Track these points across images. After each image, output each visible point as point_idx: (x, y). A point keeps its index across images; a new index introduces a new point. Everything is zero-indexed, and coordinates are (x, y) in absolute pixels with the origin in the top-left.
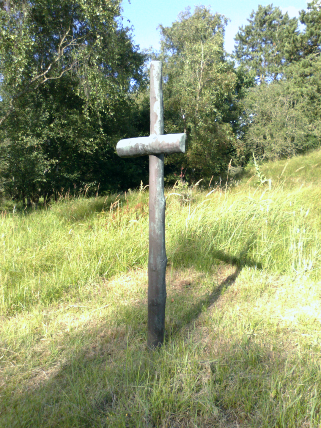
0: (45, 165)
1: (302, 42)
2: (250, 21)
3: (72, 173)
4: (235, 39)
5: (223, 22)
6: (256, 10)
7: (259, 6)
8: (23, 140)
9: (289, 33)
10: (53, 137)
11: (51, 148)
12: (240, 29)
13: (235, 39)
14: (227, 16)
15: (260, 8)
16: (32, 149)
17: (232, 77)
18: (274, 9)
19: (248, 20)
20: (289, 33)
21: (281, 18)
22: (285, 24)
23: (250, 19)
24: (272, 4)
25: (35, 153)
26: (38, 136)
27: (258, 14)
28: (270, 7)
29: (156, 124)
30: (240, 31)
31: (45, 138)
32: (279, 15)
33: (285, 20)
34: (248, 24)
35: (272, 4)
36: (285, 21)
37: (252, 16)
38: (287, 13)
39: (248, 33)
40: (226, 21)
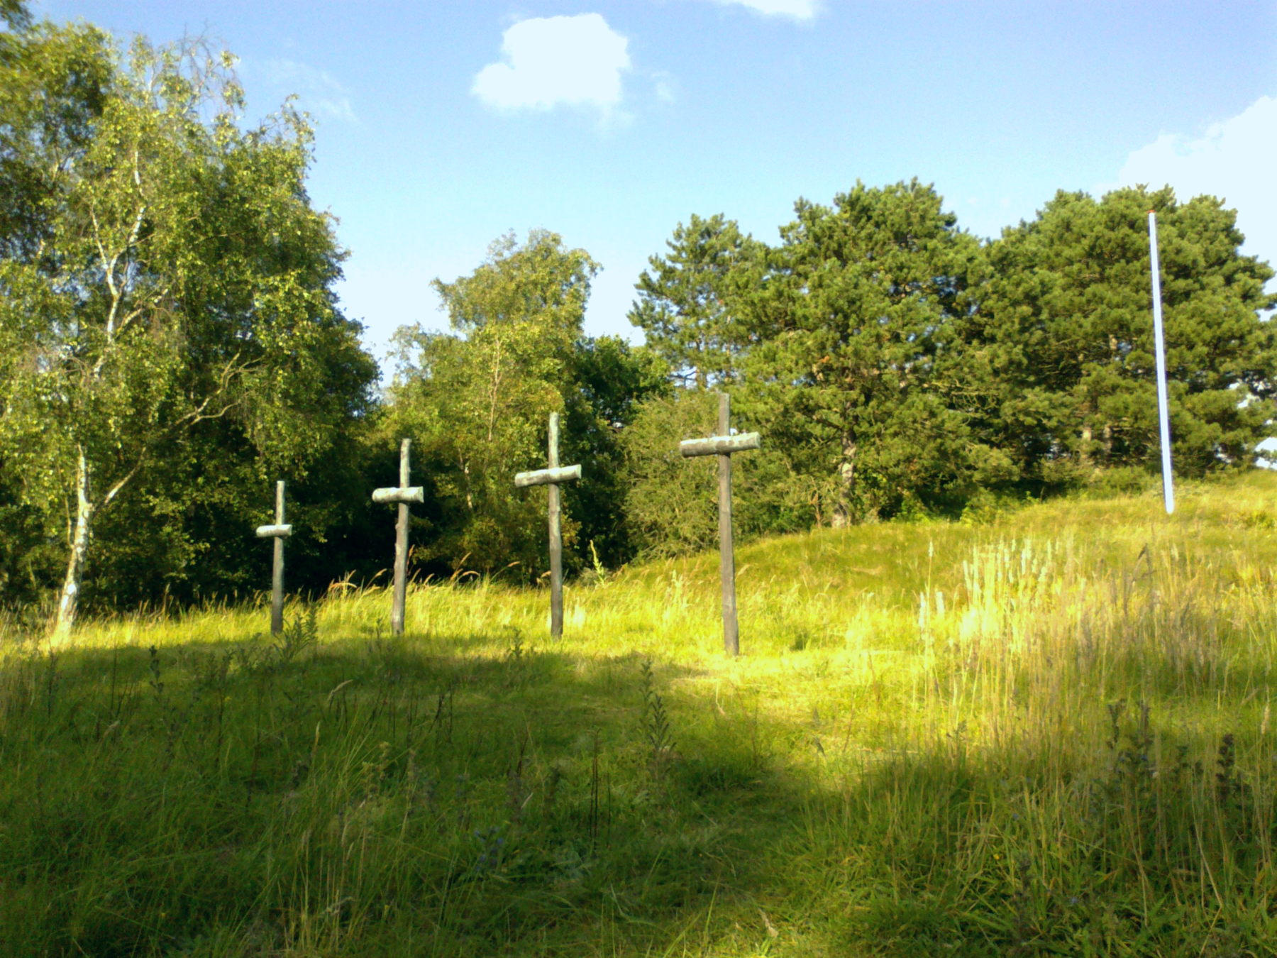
0: (185, 553)
1: (764, 307)
2: (675, 248)
3: (235, 570)
4: (638, 287)
5: (586, 270)
6: (687, 224)
7: (693, 216)
8: (148, 501)
9: (738, 287)
10: (203, 502)
11: (196, 522)
12: (652, 262)
13: (638, 287)
14: (595, 259)
15: (695, 224)
16: (163, 519)
17: (555, 400)
18: (726, 226)
19: (669, 244)
20: (738, 287)
21: (740, 246)
22: (746, 259)
23: (674, 242)
24: (722, 215)
25: (167, 529)
26: (176, 498)
27: (689, 234)
28: (717, 220)
29: (280, 518)
30: (650, 269)
31: (189, 503)
32: (735, 240)
33: (747, 251)
34: (673, 253)
35: (722, 215)
36: (747, 254)
37: (678, 236)
38: (750, 235)
39: (668, 273)
40: (593, 269)
